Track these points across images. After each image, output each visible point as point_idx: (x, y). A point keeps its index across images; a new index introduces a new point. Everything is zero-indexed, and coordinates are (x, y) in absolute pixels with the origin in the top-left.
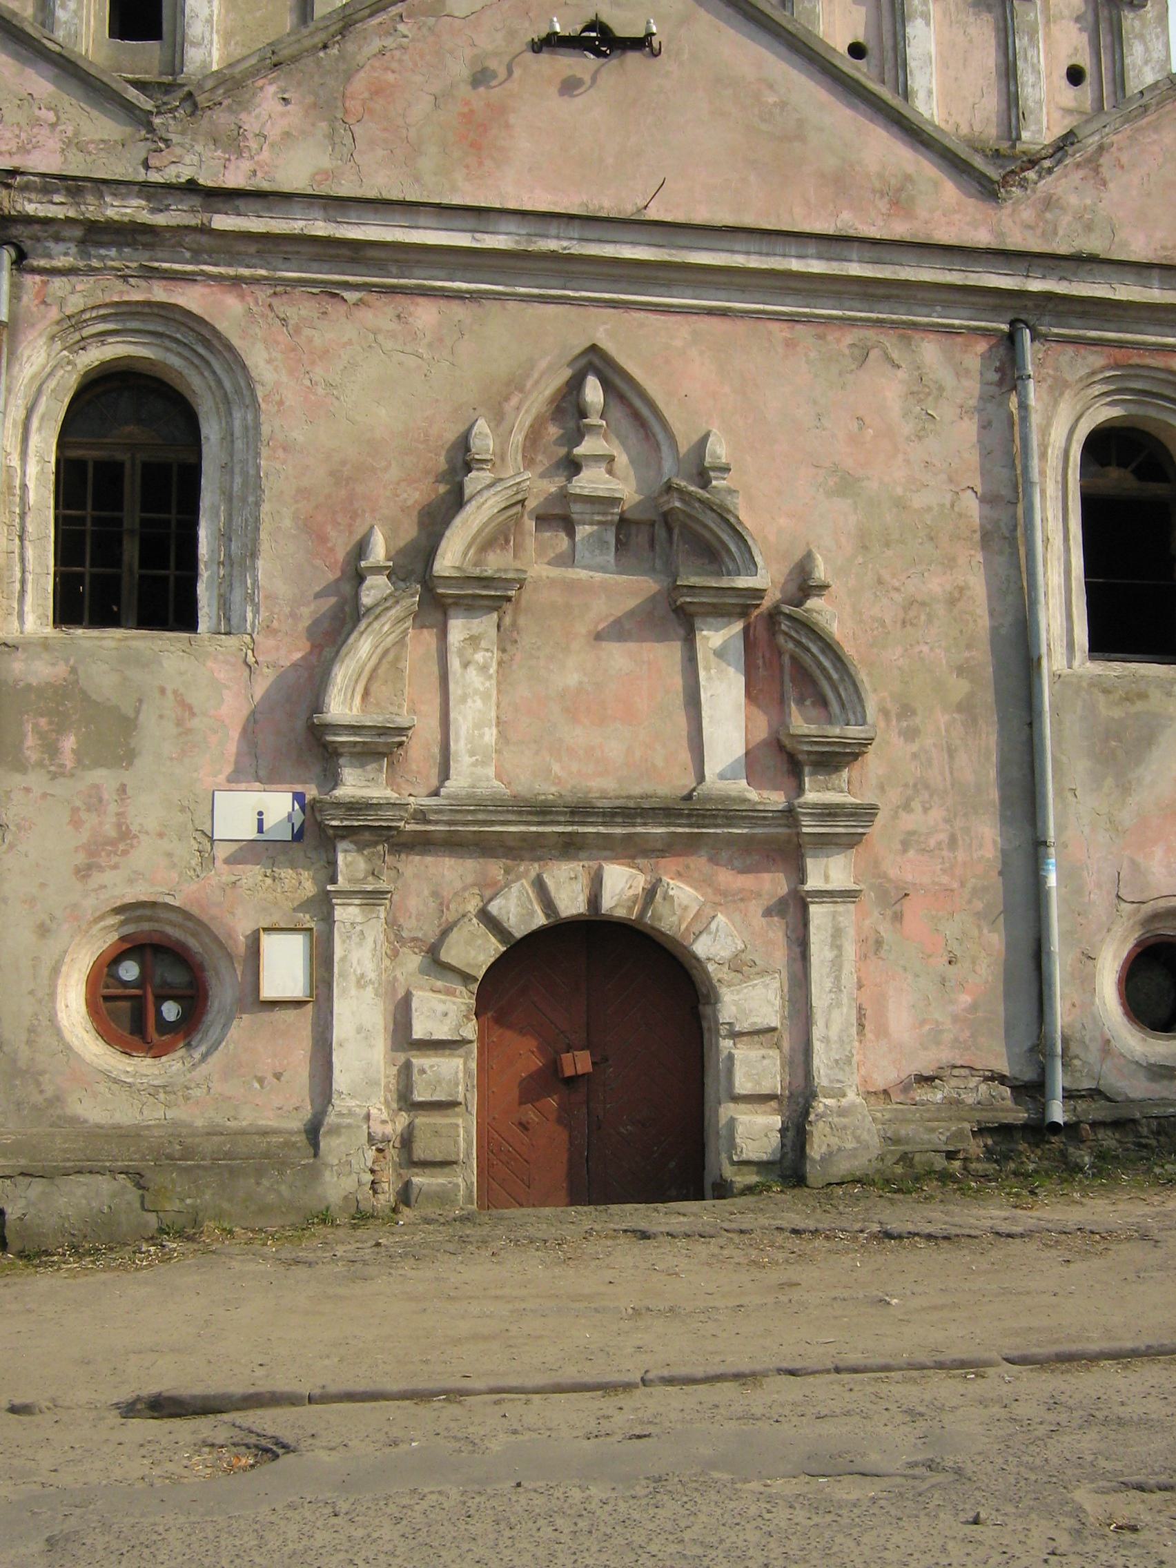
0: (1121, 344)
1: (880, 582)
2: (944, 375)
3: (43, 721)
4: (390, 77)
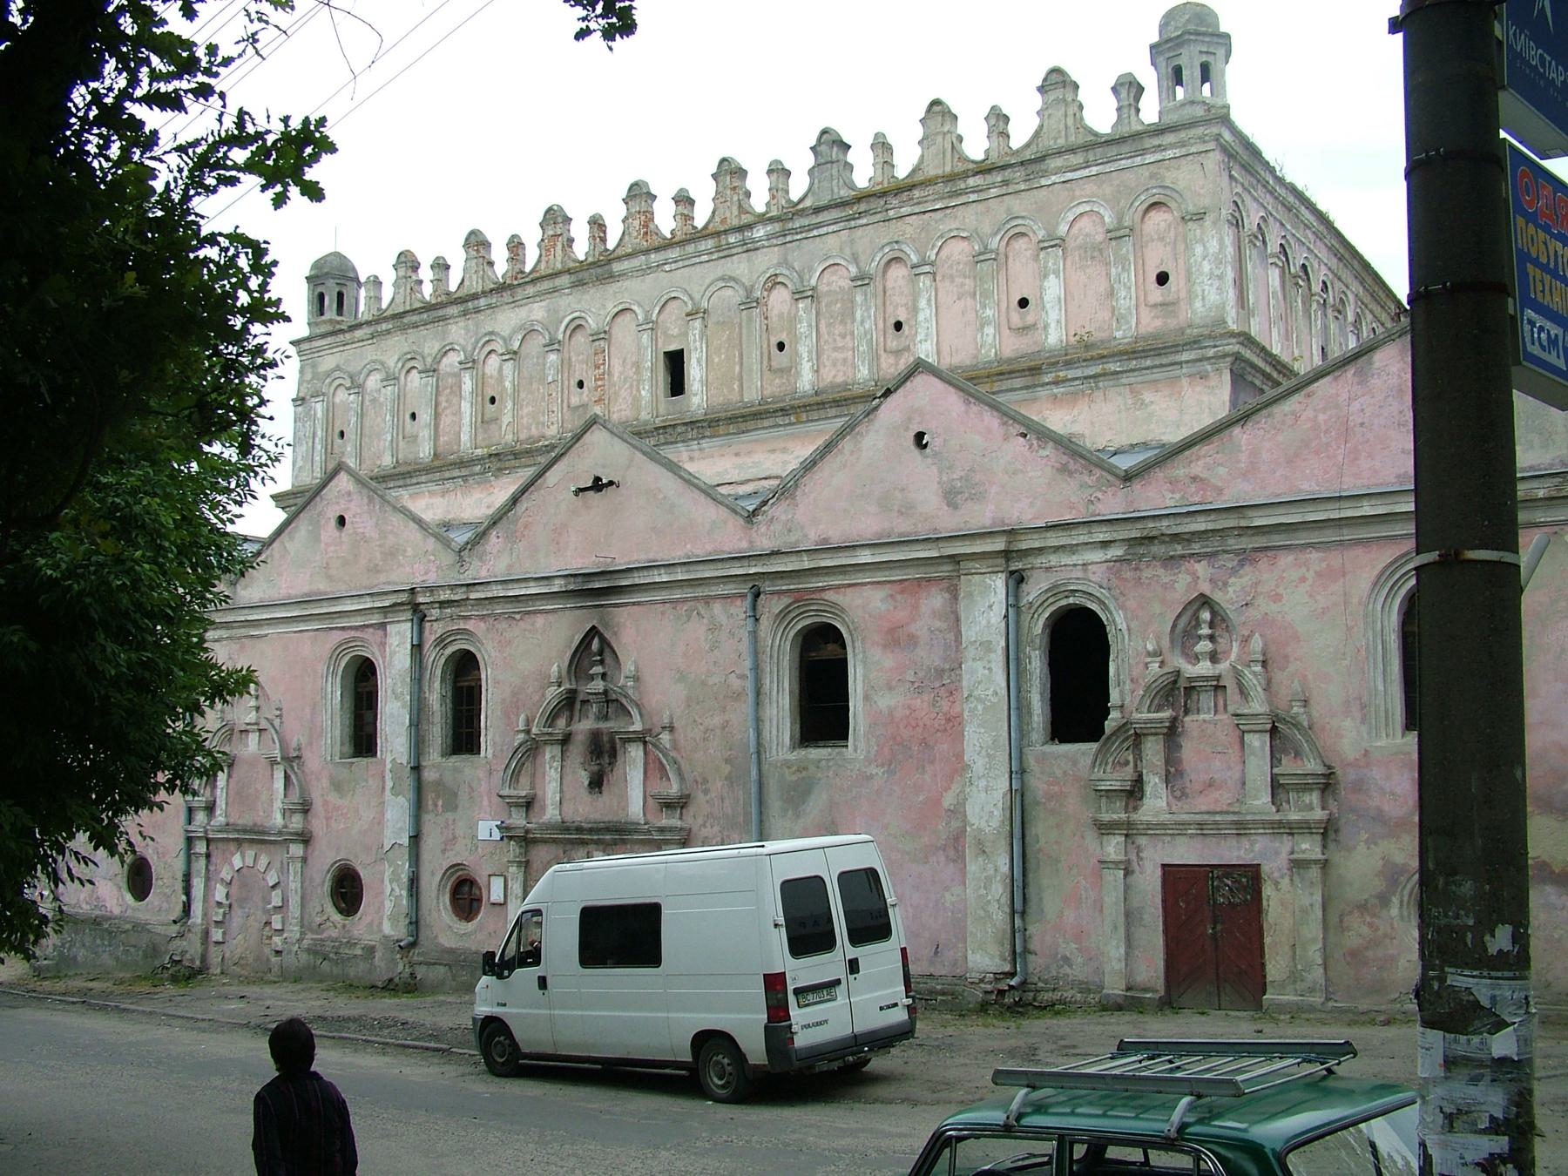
0: (798, 590)
1: (695, 721)
2: (723, 619)
3: (433, 795)
4: (530, 519)
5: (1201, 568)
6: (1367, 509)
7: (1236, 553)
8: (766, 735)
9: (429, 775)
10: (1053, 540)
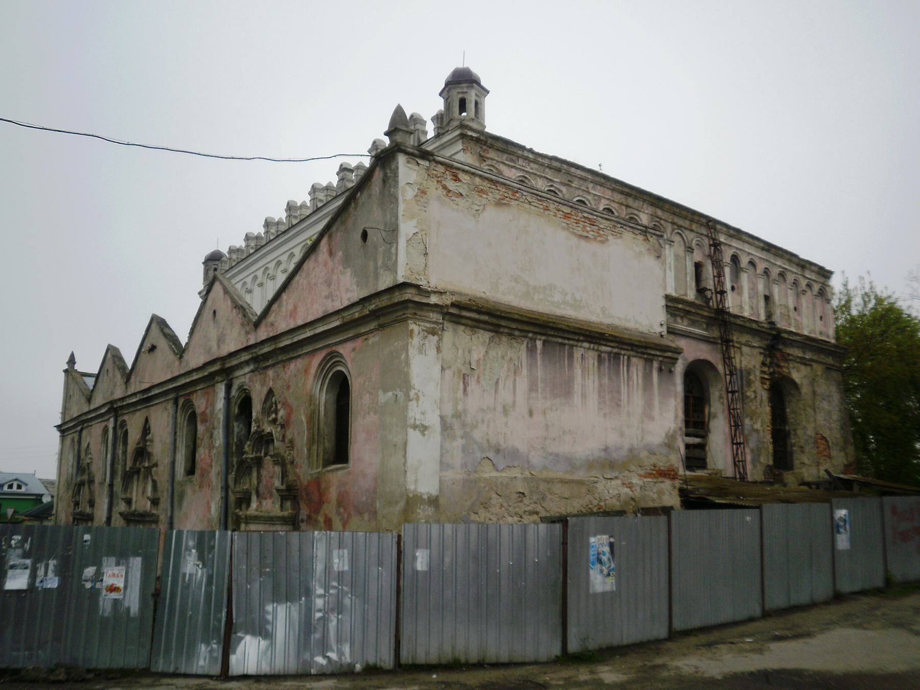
5: (270, 373)
6: (308, 333)
7: (283, 361)
8: (176, 469)
9: (115, 489)
10: (234, 362)
